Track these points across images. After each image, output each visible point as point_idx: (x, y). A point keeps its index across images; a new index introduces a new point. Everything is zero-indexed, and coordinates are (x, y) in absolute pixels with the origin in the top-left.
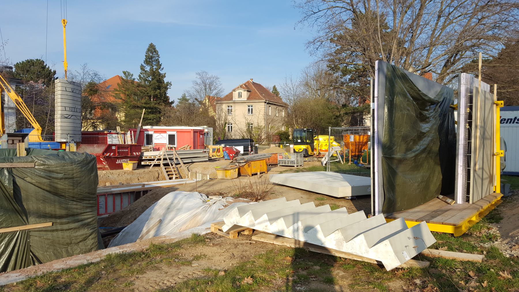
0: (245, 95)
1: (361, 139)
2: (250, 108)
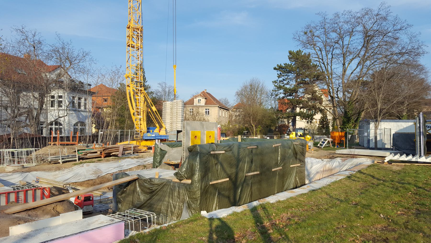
0: (203, 101)
1: (342, 134)
2: (207, 111)
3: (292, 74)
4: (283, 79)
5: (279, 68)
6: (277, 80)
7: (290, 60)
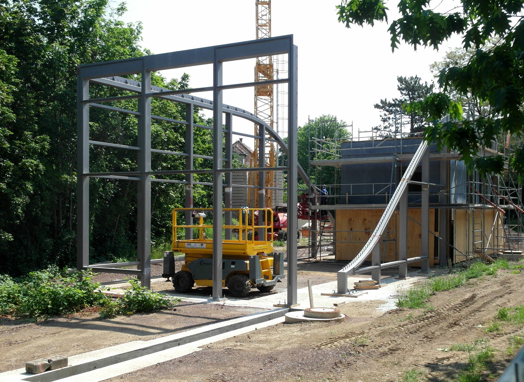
3: (405, 117)
4: (389, 124)
5: (384, 105)
6: (380, 126)
7: (402, 93)
